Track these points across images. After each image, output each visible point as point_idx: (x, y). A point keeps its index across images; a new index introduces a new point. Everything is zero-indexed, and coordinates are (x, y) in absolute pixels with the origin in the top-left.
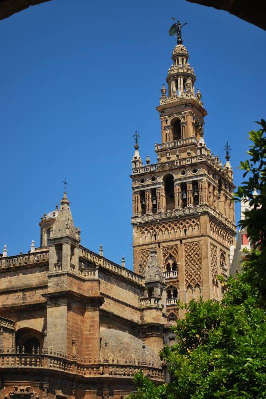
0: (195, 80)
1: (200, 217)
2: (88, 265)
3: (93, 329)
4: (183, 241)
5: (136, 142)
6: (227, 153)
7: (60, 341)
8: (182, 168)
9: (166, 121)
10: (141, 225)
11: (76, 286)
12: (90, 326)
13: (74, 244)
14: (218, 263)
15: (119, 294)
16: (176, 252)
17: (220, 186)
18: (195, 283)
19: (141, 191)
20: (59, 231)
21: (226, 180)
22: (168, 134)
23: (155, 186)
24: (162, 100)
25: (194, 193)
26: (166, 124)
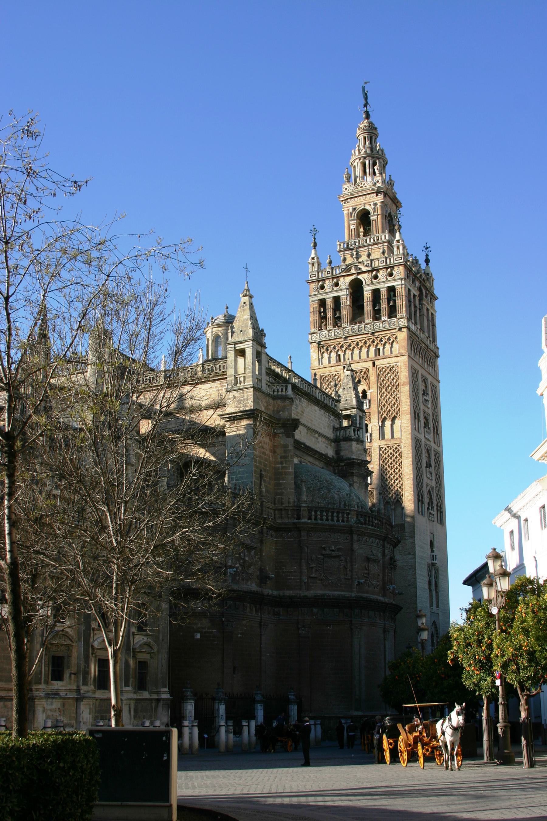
0: (386, 164)
3: (285, 461)
4: (377, 363)
5: (315, 239)
6: (427, 255)
7: (246, 475)
9: (351, 214)
11: (263, 405)
12: (281, 458)
13: (260, 350)
14: (421, 393)
15: (311, 420)
16: (367, 376)
17: (421, 295)
18: (393, 415)
19: (321, 300)
22: (353, 230)
24: (346, 186)
26: (351, 217)
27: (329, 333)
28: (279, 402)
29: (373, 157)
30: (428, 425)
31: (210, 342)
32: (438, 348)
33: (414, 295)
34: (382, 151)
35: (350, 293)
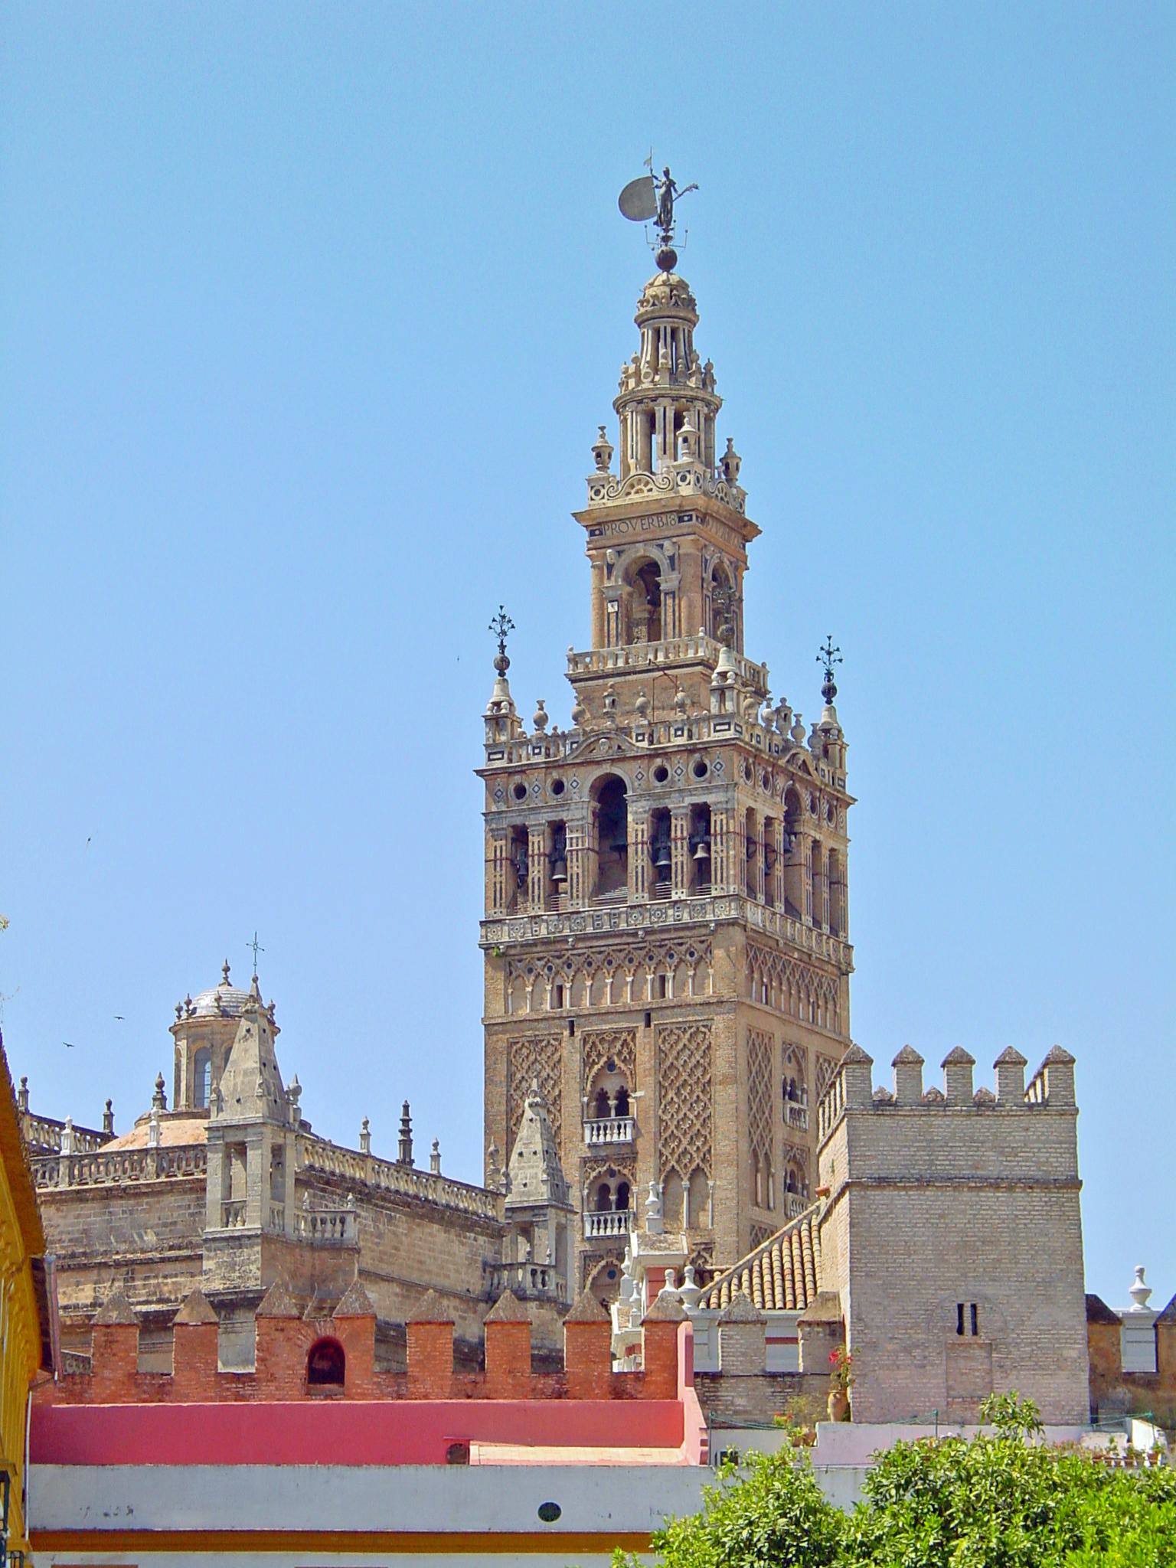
1: (713, 933)
2: (323, 1190)
5: (502, 647)
6: (829, 674)
8: (658, 755)
9: (610, 567)
10: (513, 952)
13: (280, 1141)
14: (777, 1090)
15: (421, 1262)
16: (630, 1053)
18: (694, 1166)
20: (238, 1101)
21: (811, 785)
22: (613, 618)
23: (564, 816)
25: (693, 850)
27: (536, 921)
28: (325, 1255)
29: (675, 399)
30: (803, 1179)
31: (184, 1061)
32: (849, 947)
33: (769, 821)
34: (709, 366)
35: (594, 813)
